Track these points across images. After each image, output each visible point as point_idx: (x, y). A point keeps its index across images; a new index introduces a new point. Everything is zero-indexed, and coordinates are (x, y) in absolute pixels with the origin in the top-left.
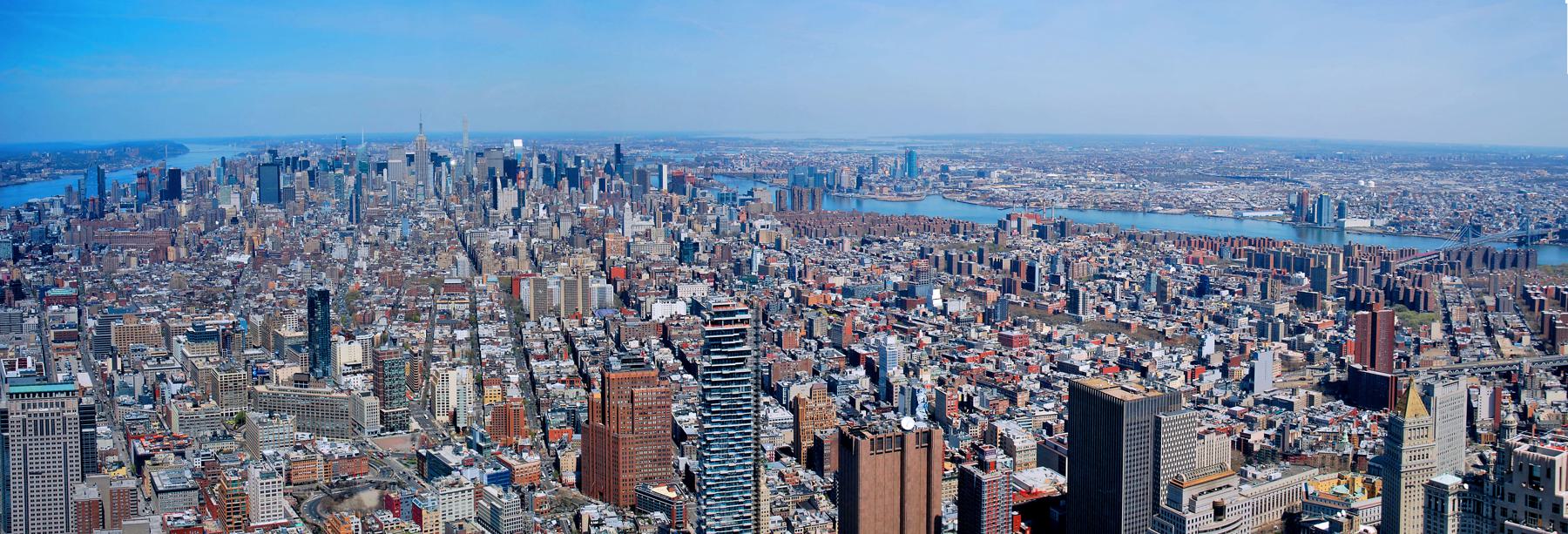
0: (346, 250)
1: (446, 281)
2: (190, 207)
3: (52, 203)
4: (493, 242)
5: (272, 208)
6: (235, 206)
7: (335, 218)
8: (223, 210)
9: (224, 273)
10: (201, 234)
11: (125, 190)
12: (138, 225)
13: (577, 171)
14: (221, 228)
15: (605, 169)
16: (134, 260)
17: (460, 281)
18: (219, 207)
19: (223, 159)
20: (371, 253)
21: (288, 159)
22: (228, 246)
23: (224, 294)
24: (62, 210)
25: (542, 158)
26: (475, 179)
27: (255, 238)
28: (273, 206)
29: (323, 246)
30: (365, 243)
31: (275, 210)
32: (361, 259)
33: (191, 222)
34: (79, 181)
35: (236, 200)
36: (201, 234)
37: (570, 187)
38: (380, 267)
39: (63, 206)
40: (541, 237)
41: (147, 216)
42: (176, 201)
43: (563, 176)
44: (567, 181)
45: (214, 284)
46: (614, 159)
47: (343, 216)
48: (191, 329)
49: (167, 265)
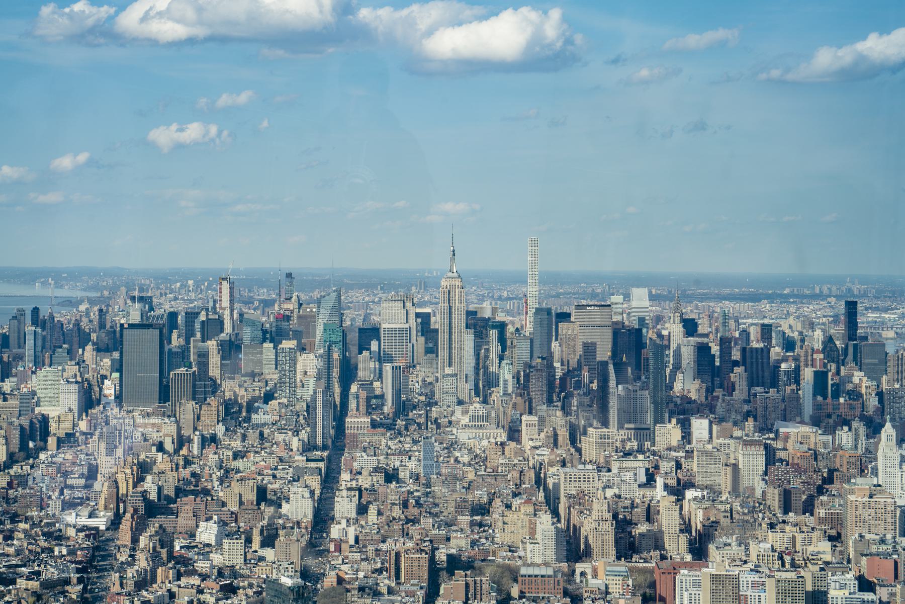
0: (310, 502)
1: (523, 571)
4: (609, 493)
5: (148, 415)
6: (70, 410)
7: (280, 437)
13: (766, 351)
14: (42, 456)
15: (823, 351)
17: (550, 572)
19: (36, 311)
20: (362, 510)
21: (173, 316)
22: (62, 493)
25: (690, 327)
26: (557, 365)
27: (120, 477)
28: (149, 410)
29: (262, 494)
30: (350, 489)
31: (155, 420)
32: (344, 522)
35: (70, 398)
37: (752, 383)
38: (384, 541)
40: (702, 489)
43: (736, 363)
44: (745, 375)
45: (38, 574)
46: (838, 331)
47: (296, 433)
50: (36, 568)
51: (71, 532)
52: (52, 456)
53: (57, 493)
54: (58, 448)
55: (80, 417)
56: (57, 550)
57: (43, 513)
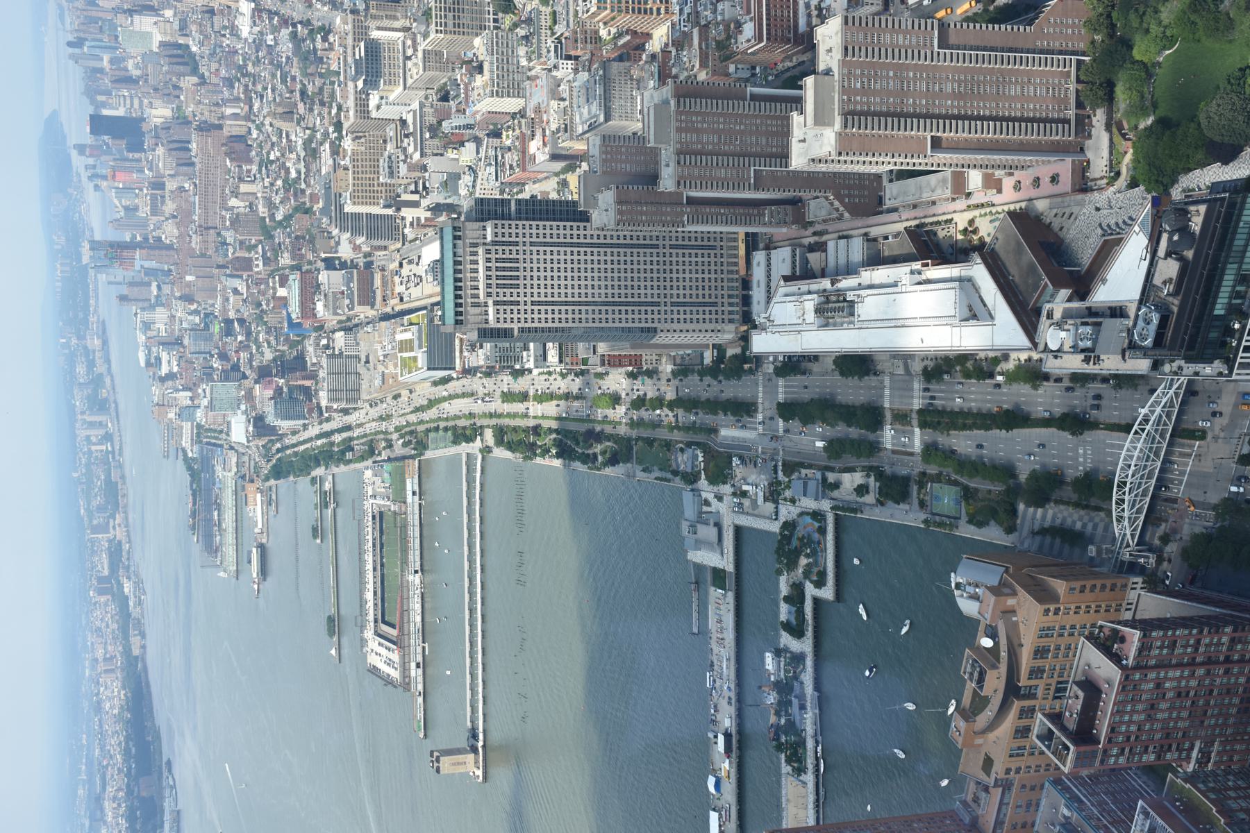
2: (157, 103)
3: (147, 326)
8: (163, 44)
9: (270, 40)
10: (203, 81)
11: (126, 208)
12: (186, 186)
14: (194, 49)
16: (244, 188)
18: (155, 50)
22: (224, 36)
23: (304, 40)
24: (159, 310)
33: (182, 98)
34: (110, 283)
36: (203, 81)
39: (152, 307)
41: (172, 172)
42: (145, 127)
45: (288, 58)
48: (360, 84)
49: (255, 136)
50: (284, 59)
51: (256, 29)
52: (194, 40)
53: (224, 39)
54: (186, 35)
55: (163, 16)
56: (269, 43)
57: (240, 52)
